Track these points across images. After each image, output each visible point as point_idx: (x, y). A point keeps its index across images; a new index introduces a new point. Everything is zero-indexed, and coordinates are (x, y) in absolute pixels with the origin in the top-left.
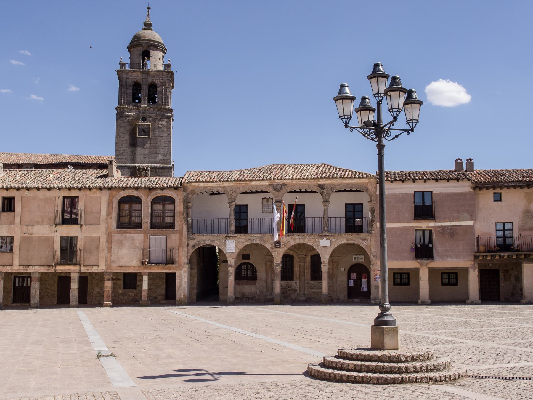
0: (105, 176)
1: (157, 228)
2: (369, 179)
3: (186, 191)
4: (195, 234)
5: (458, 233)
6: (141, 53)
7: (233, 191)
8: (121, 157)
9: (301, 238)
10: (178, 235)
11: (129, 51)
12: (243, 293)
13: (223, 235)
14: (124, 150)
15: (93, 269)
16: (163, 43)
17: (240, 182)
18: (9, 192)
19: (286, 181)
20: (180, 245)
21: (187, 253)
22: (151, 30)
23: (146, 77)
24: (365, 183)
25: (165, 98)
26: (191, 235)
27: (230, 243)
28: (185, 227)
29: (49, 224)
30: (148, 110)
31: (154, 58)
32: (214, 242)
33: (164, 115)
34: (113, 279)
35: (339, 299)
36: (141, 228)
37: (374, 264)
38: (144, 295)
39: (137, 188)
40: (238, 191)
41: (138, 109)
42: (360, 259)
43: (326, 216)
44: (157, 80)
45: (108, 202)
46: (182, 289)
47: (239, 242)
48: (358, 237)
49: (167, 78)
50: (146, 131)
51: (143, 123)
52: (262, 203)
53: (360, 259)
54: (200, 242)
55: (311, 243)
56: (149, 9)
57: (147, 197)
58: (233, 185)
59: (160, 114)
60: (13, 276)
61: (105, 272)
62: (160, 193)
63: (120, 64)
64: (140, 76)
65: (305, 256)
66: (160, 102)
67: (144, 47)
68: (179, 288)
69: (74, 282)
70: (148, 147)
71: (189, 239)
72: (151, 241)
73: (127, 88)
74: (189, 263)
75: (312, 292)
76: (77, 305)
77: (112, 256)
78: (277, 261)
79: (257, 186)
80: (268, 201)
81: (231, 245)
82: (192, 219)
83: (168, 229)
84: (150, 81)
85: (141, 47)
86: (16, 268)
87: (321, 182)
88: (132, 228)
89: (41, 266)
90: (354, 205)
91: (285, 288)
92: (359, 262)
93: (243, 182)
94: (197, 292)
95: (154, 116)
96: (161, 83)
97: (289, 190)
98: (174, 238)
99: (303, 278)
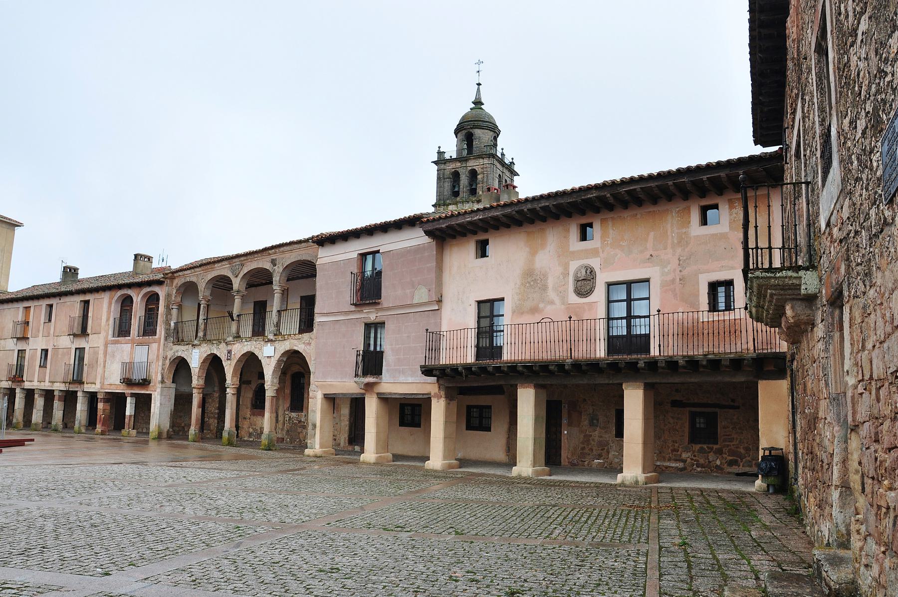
56: (479, 84)
83: (150, 337)
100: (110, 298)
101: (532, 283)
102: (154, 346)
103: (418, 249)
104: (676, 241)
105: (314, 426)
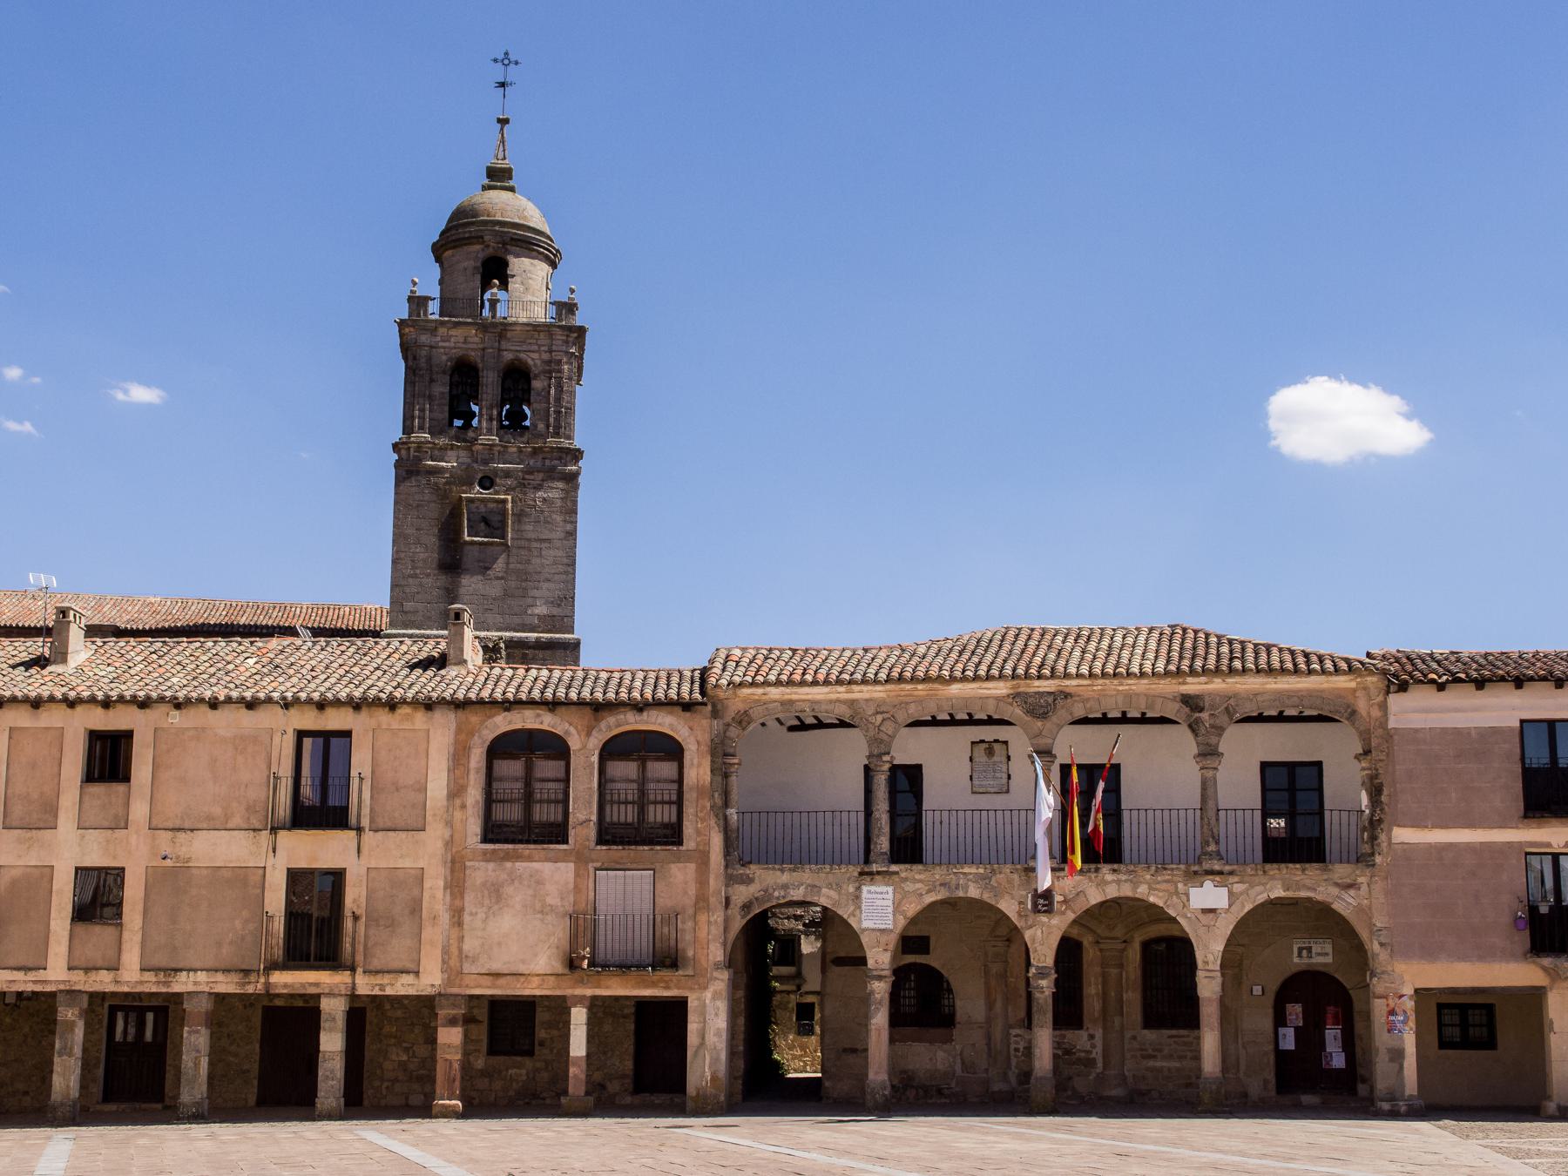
0: (440, 662)
1: (622, 843)
2: (1360, 676)
3: (720, 713)
4: (750, 863)
6: (479, 264)
7: (886, 715)
8: (408, 606)
9: (1126, 881)
10: (692, 867)
11: (438, 259)
12: (904, 1072)
13: (851, 868)
14: (421, 585)
15: (399, 984)
16: (548, 231)
17: (909, 687)
18: (111, 712)
19: (1067, 682)
20: (701, 902)
21: (726, 930)
22: (512, 189)
24: (1346, 689)
25: (558, 413)
26: (738, 866)
27: (874, 896)
28: (717, 841)
29: (246, 826)
30: (499, 452)
32: (819, 892)
33: (552, 469)
34: (468, 1020)
35: (1245, 1095)
36: (567, 843)
37: (1383, 972)
38: (575, 1075)
39: (553, 705)
40: (903, 717)
41: (469, 449)
42: (1319, 954)
43: (1211, 804)
45: (452, 750)
46: (707, 1057)
47: (905, 894)
48: (1325, 877)
49: (564, 348)
50: (492, 523)
51: (486, 494)
52: (971, 759)
53: (1319, 954)
54: (771, 891)
55: (1160, 898)
56: (504, 122)
57: (589, 734)
59: (539, 464)
60: (106, 1005)
61: (440, 994)
62: (633, 722)
63: (410, 299)
65: (1125, 942)
66: (541, 426)
69: (331, 1030)
70: (500, 575)
71: (730, 880)
72: (601, 888)
73: (432, 381)
74: (730, 967)
75: (1147, 1069)
76: (340, 1113)
77: (466, 939)
78: (1043, 958)
79: (967, 700)
80: (990, 752)
81: (879, 902)
82: (741, 813)
83: (659, 848)
84: (508, 356)
85: (478, 247)
86: (131, 976)
87: (1193, 686)
88: (535, 842)
89: (216, 971)
90: (1291, 767)
92: (1312, 963)
93: (920, 687)
94: (746, 1064)
95: (522, 470)
96: (544, 362)
97: (1079, 712)
98: (680, 877)
99: (1117, 1020)
105: (1397, 1055)
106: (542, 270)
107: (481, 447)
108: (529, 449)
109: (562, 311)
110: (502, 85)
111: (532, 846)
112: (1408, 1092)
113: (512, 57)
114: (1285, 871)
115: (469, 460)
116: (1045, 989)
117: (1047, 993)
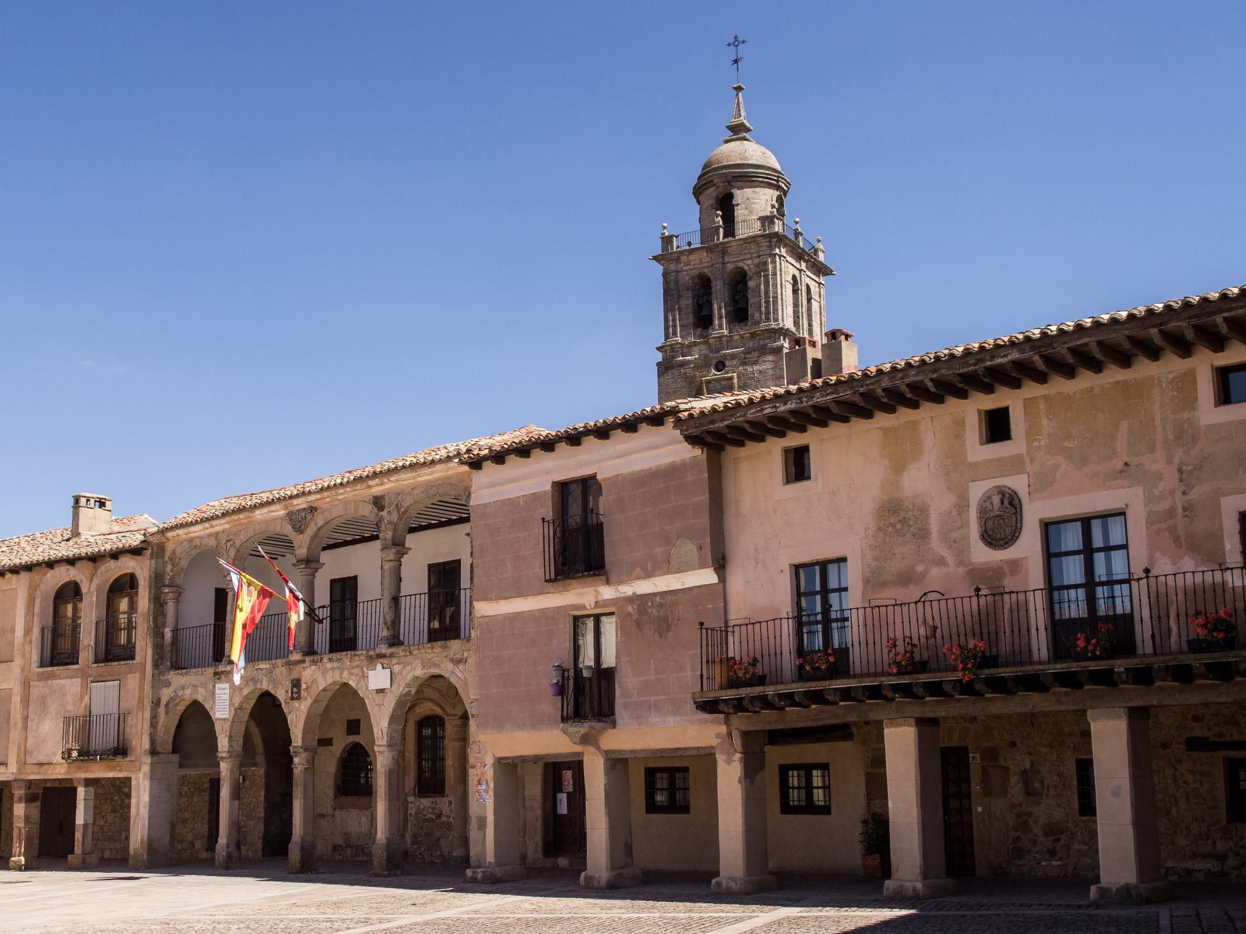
5: (679, 619)
12: (346, 834)
21: (153, 725)
23: (721, 260)
25: (767, 302)
30: (728, 342)
31: (747, 209)
36: (77, 663)
41: (707, 343)
44: (744, 262)
48: (445, 654)
49: (768, 252)
56: (739, 89)
57: (91, 581)
58: (227, 526)
64: (708, 259)
66: (757, 315)
67: (718, 187)
68: (134, 822)
73: (680, 297)
83: (122, 663)
84: (730, 267)
85: (713, 189)
87: (377, 488)
91: (430, 820)
95: (743, 352)
100: (30, 588)
101: (899, 526)
102: (132, 680)
103: (670, 473)
104: (1171, 437)
105: (482, 822)
106: (765, 194)
107: (713, 340)
108: (748, 335)
109: (765, 223)
110: (736, 61)
111: (61, 668)
112: (488, 861)
113: (740, 39)
114: (423, 651)
115: (706, 352)
116: (297, 766)
117: (299, 769)
